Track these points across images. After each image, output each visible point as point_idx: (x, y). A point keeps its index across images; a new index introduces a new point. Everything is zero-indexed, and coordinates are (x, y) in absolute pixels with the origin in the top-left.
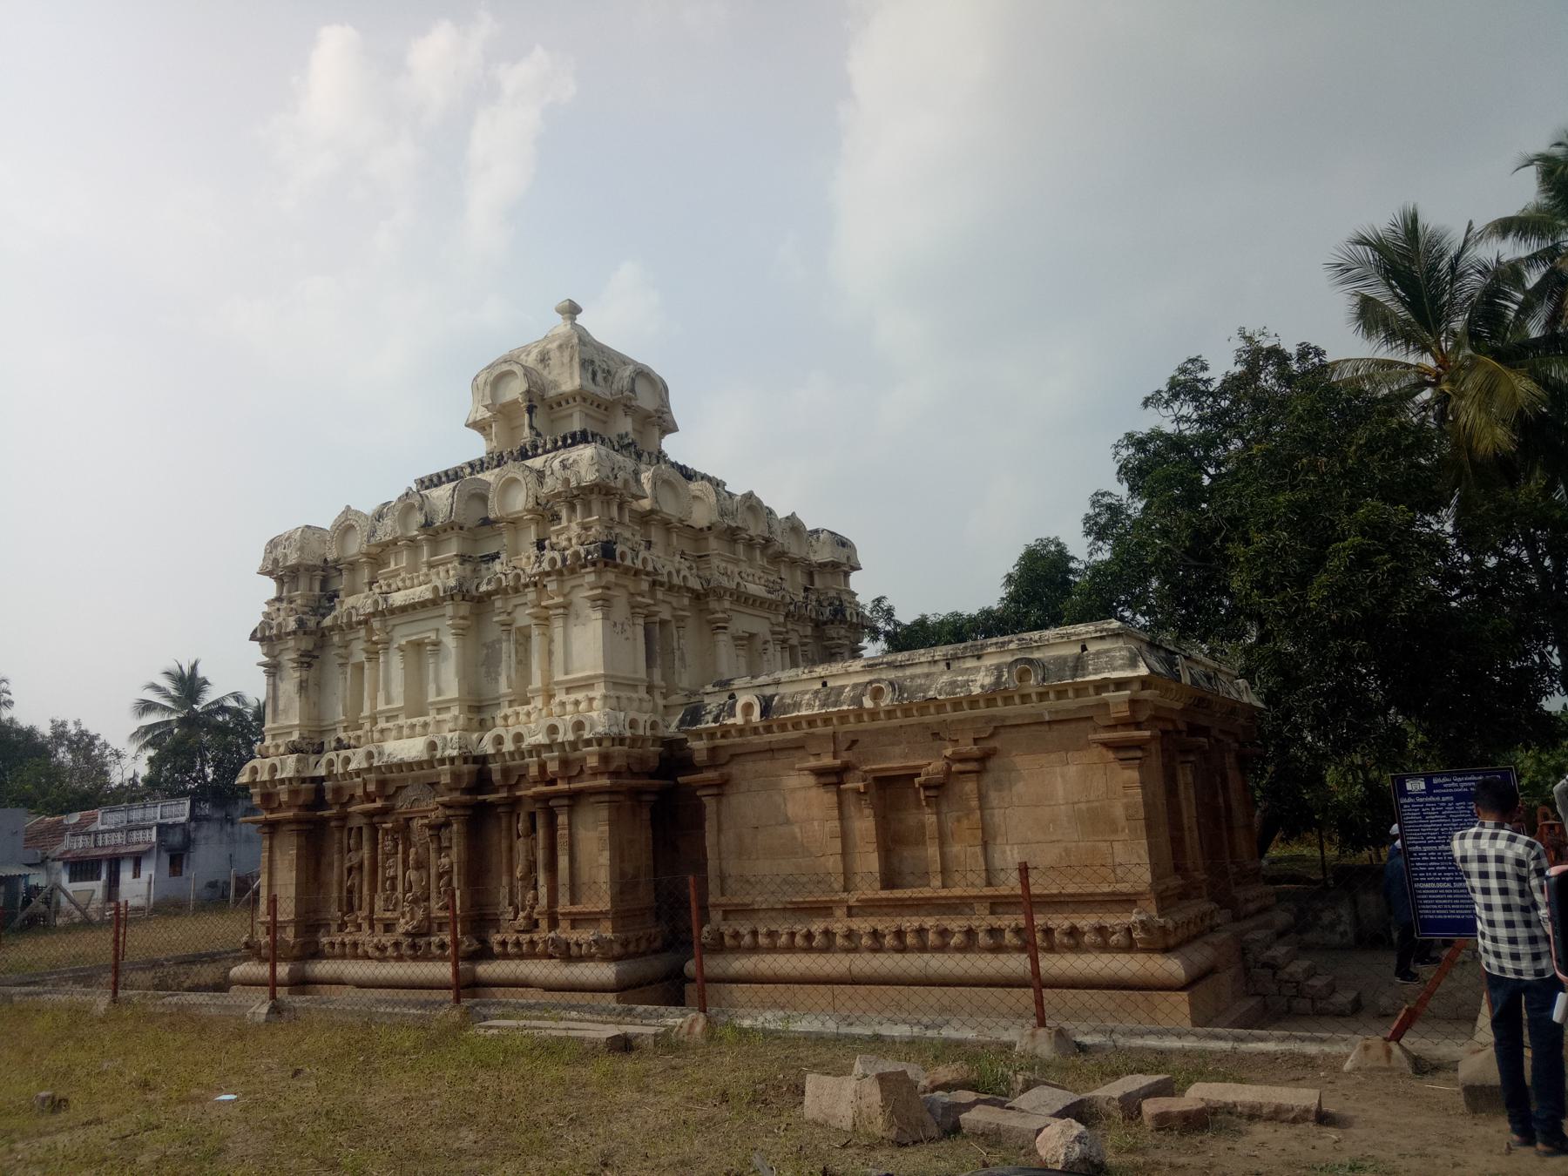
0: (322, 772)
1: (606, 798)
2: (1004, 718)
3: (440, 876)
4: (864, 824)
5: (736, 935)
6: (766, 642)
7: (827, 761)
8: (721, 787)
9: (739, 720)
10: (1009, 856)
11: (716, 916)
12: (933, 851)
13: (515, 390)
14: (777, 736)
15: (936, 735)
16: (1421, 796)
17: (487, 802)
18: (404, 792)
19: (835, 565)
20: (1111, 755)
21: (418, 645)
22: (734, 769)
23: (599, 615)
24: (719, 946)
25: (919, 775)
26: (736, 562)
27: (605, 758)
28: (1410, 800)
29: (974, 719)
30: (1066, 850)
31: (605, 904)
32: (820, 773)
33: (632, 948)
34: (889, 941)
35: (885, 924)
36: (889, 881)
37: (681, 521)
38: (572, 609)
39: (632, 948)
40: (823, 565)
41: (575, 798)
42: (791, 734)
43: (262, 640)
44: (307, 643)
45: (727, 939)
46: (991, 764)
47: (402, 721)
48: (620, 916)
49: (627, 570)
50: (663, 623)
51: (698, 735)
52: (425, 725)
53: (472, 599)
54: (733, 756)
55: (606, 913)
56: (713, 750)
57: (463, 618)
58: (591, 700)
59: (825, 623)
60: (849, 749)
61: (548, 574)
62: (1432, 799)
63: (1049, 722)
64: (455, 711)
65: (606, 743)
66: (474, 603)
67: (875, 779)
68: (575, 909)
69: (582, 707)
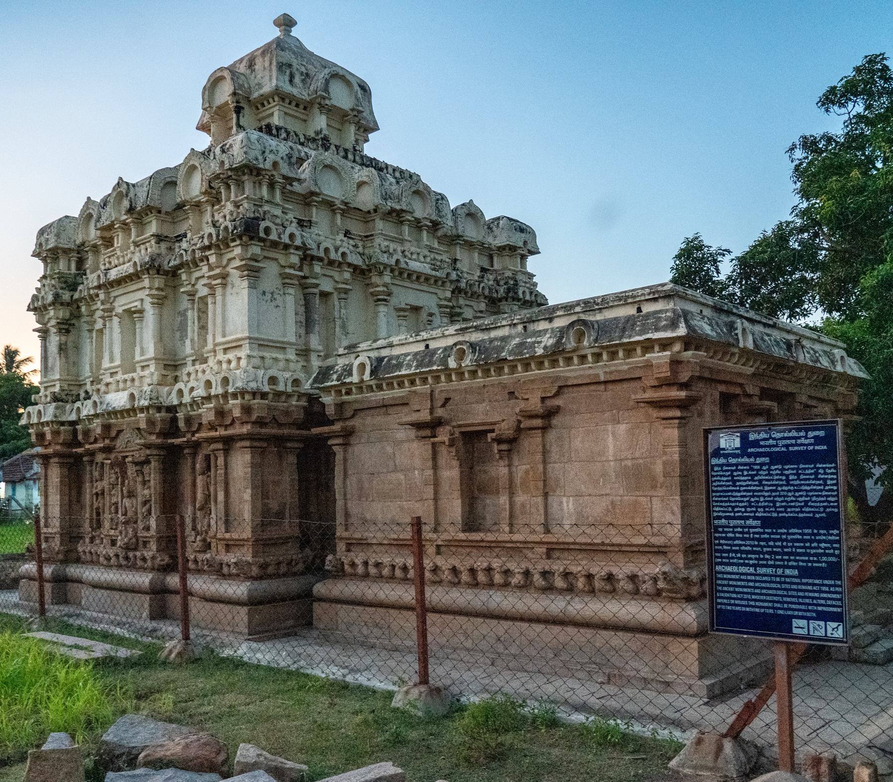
0: (73, 417)
1: (247, 443)
2: (567, 378)
4: (451, 473)
5: (353, 565)
6: (431, 315)
7: (425, 416)
8: (348, 434)
9: (355, 378)
10: (566, 507)
11: (341, 546)
12: (504, 499)
13: (224, 94)
14: (387, 394)
15: (511, 393)
16: (735, 456)
17: (175, 444)
18: (122, 435)
19: (512, 249)
20: (655, 413)
21: (129, 312)
22: (356, 422)
23: (245, 284)
24: (339, 573)
25: (493, 431)
26: (402, 241)
27: (247, 410)
28: (722, 461)
29: (543, 380)
30: (612, 503)
31: (247, 534)
32: (418, 426)
33: (270, 570)
34: (465, 577)
35: (462, 562)
36: (471, 523)
37: (346, 204)
38: (229, 279)
39: (270, 570)
40: (501, 249)
41: (228, 443)
42: (397, 392)
43: (35, 309)
44: (63, 313)
45: (346, 567)
46: (555, 421)
47: (119, 377)
48: (261, 543)
49: (275, 245)
50: (325, 295)
51: (327, 390)
52: (133, 380)
53: (166, 273)
54: (356, 411)
55: (247, 540)
56: (340, 406)
57: (158, 289)
58: (239, 359)
59: (500, 300)
60: (443, 406)
61: (209, 248)
62: (745, 460)
63: (605, 382)
64: (152, 368)
65: (247, 397)
66: (167, 275)
67: (462, 433)
68: (227, 536)
69: (233, 364)
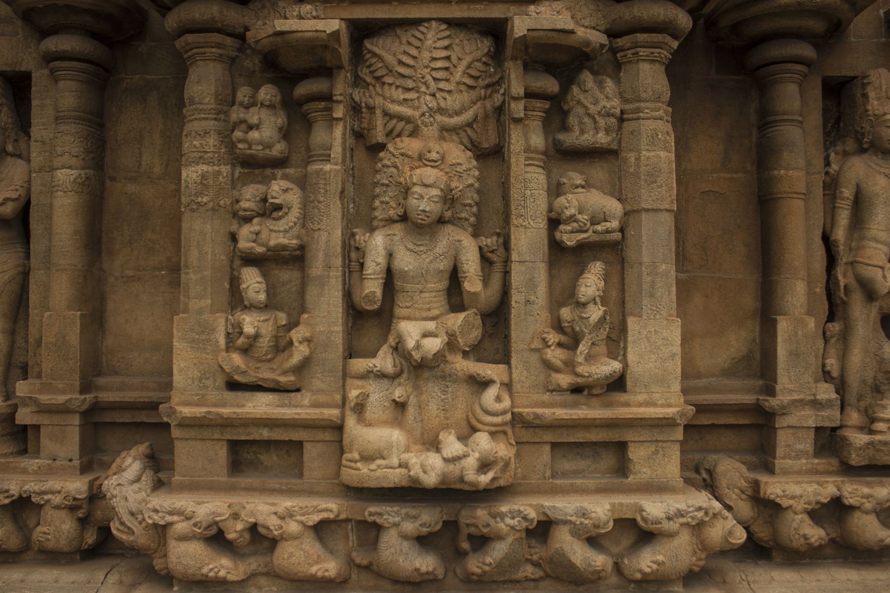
3: (565, 257)
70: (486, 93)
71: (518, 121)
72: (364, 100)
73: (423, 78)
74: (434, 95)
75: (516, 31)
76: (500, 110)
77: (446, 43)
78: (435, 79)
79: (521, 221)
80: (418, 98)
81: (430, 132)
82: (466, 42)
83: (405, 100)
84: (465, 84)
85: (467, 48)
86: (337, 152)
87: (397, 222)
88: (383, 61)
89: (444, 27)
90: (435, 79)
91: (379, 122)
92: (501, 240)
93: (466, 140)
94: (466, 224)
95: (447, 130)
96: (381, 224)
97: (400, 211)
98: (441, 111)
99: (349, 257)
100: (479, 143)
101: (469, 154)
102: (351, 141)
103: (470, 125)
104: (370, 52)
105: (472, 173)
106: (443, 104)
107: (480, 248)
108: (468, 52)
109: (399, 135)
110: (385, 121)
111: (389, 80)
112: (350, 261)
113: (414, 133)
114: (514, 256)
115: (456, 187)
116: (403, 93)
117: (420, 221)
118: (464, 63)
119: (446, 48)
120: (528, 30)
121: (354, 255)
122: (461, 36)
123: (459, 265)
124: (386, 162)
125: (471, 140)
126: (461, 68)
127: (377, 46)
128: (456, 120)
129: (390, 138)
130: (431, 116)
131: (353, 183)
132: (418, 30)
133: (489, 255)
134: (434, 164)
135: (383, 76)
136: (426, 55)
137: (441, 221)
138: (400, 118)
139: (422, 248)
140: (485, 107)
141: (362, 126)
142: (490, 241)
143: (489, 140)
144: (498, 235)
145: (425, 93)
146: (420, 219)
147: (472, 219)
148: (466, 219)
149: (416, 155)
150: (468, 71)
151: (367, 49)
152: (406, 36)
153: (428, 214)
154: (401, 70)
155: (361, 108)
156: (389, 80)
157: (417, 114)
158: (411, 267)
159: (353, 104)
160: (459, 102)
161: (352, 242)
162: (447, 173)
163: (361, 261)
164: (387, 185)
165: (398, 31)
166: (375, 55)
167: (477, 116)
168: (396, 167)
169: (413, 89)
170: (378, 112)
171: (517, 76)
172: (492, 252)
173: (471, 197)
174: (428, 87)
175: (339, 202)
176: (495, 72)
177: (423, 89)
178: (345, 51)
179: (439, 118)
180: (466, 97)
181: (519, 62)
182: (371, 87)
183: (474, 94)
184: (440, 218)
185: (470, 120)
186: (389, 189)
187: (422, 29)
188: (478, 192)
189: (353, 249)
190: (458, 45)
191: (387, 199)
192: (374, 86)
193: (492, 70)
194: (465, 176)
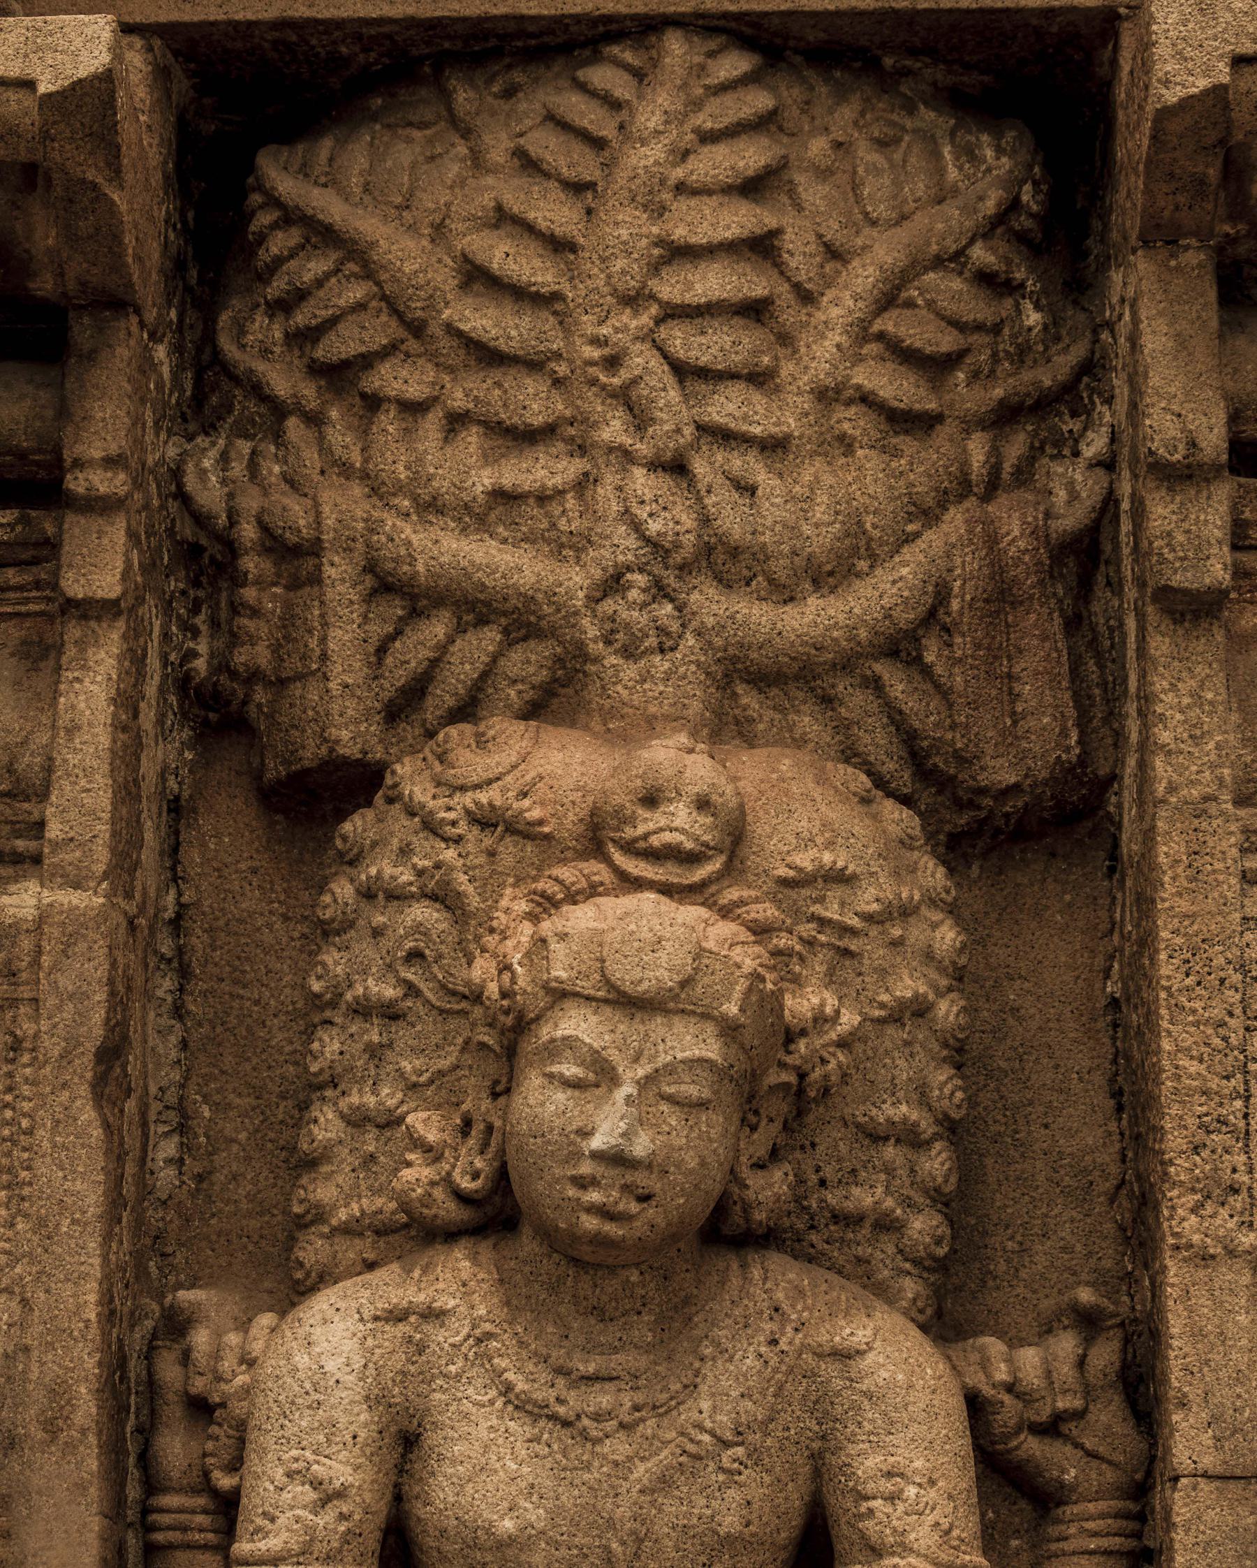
70: (995, 454)
71: (1194, 609)
72: (250, 502)
73: (613, 362)
74: (677, 467)
75: (1165, 63)
76: (1084, 558)
77: (751, 156)
78: (682, 371)
79: (1224, 1222)
80: (583, 484)
81: (669, 679)
82: (867, 155)
83: (503, 497)
84: (866, 399)
85: (877, 193)
86: (82, 805)
87: (449, 1235)
88: (369, 272)
89: (734, 64)
90: (682, 371)
91: (344, 628)
92: (1105, 1355)
93: (876, 740)
94: (883, 1253)
95: (762, 679)
96: (350, 1250)
97: (469, 1169)
98: (722, 560)
99: (145, 1459)
100: (961, 759)
101: (898, 819)
102: (165, 753)
103: (900, 646)
104: (291, 216)
105: (916, 934)
106: (732, 519)
107: (975, 1405)
108: (881, 210)
109: (467, 710)
110: (378, 630)
111: (401, 379)
112: (152, 1486)
113: (550, 703)
114: (1190, 1442)
115: (821, 1020)
116: (488, 459)
117: (590, 1223)
118: (864, 277)
119: (751, 188)
120: (1239, 61)
121: (176, 1449)
122: (834, 125)
123: (839, 1504)
124: (384, 867)
125: (909, 738)
126: (840, 307)
127: (332, 182)
128: (814, 618)
129: (410, 732)
130: (660, 591)
131: (178, 1012)
132: (583, 87)
133: (1032, 1447)
134: (689, 873)
135: (367, 361)
136: (626, 229)
137: (727, 1231)
138: (474, 606)
139: (603, 1399)
140: (992, 540)
141: (241, 657)
142: (1038, 1364)
143: (1022, 743)
144: (1089, 1322)
145: (627, 456)
146: (586, 1209)
147: (923, 1226)
148: (886, 1225)
149: (569, 823)
150: (886, 323)
151: (274, 201)
152: (517, 120)
153: (641, 1179)
154: (484, 320)
155: (231, 548)
156: (401, 379)
157: (575, 580)
158: (536, 1515)
159: (187, 530)
160: (837, 511)
161: (169, 1371)
162: (761, 931)
163: (225, 1482)
164: (391, 1014)
165: (463, 97)
166: (323, 235)
167: (942, 594)
168: (444, 897)
169: (549, 431)
170: (338, 571)
171: (1181, 342)
172: (1052, 1428)
173: (909, 1088)
174: (640, 420)
175: (87, 1114)
176: (1052, 332)
177: (614, 429)
178: (140, 206)
179: (709, 602)
180: (871, 479)
181: (1194, 257)
182: (294, 427)
183: (923, 462)
184: (721, 1208)
185: (906, 618)
186: (403, 1035)
187: (601, 76)
188: (958, 1053)
189: (173, 1411)
190: (824, 174)
191: (389, 1096)
192: (315, 420)
193: (1033, 318)
194: (873, 950)
